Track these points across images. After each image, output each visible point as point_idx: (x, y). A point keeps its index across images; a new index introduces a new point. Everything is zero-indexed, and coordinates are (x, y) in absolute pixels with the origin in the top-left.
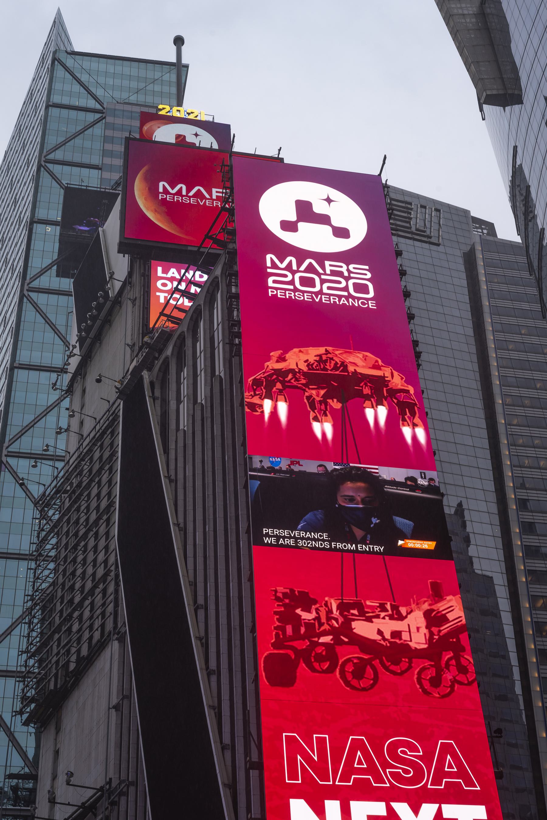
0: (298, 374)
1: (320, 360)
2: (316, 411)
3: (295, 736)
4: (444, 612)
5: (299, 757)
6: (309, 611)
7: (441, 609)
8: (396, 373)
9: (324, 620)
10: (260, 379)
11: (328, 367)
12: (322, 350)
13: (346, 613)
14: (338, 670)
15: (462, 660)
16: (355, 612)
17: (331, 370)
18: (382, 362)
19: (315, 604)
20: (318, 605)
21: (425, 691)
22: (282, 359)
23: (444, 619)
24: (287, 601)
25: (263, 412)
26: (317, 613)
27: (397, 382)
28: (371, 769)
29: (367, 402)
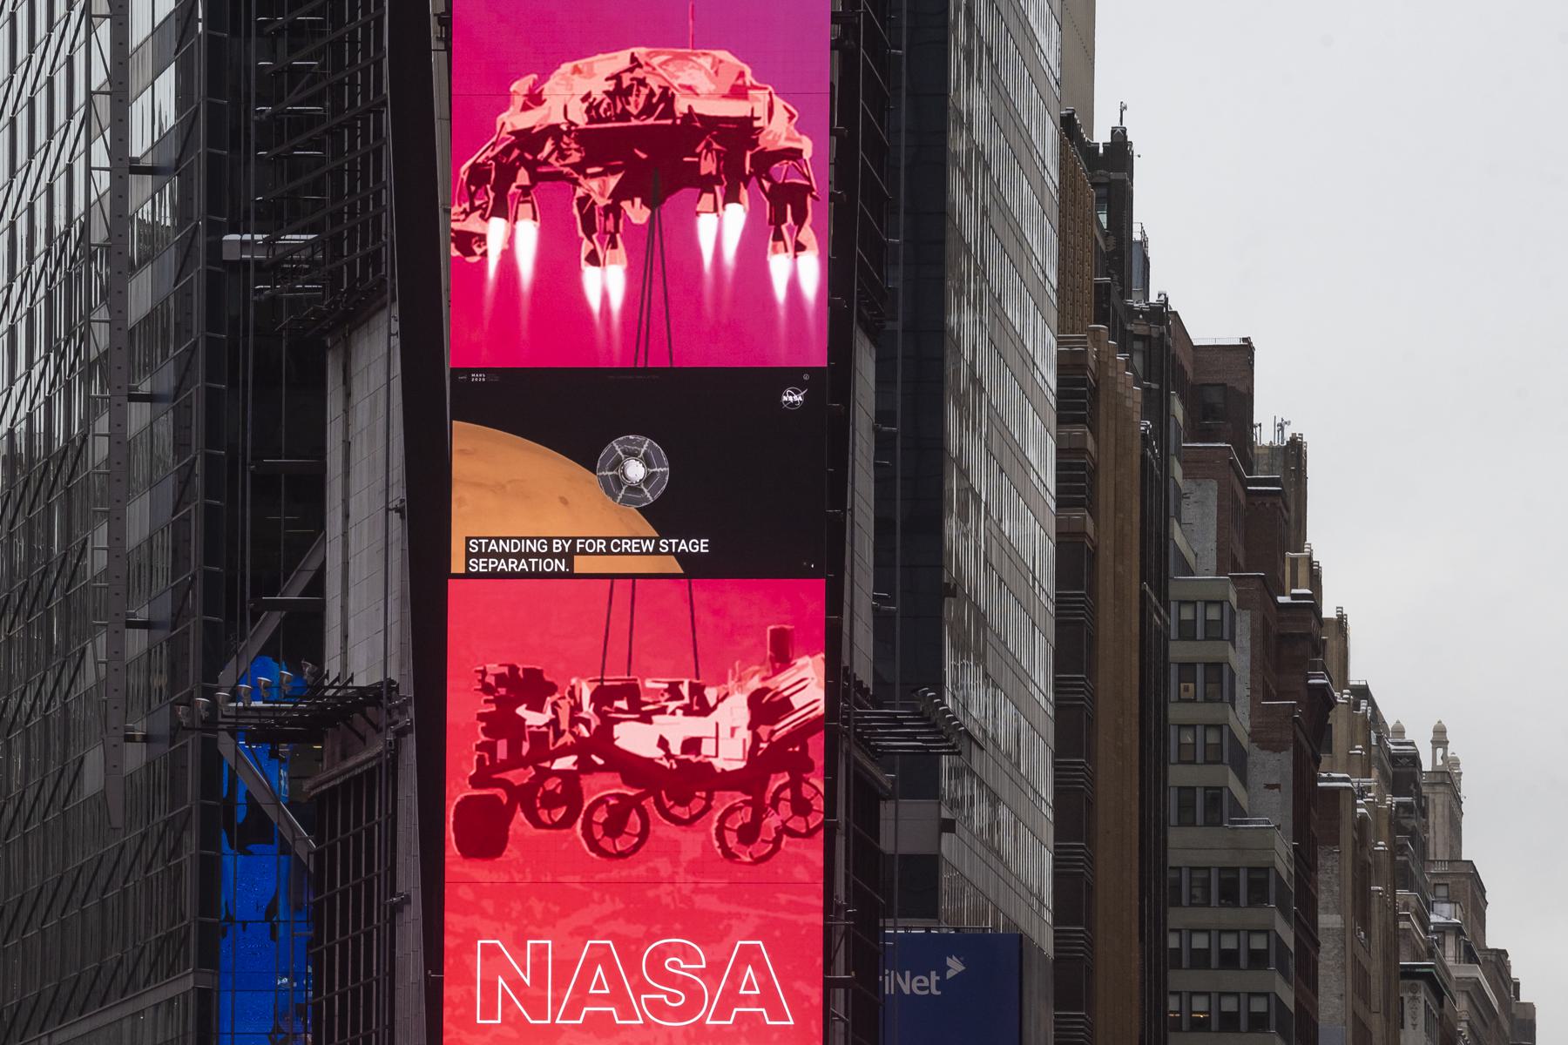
0: (566, 139)
1: (619, 92)
2: (594, 237)
3: (495, 945)
4: (786, 693)
5: (501, 981)
6: (537, 707)
7: (783, 687)
8: (779, 103)
9: (564, 725)
10: (484, 164)
11: (632, 109)
12: (621, 60)
13: (606, 708)
14: (579, 821)
15: (805, 788)
16: (622, 704)
17: (637, 117)
18: (753, 74)
19: (551, 694)
20: (557, 695)
21: (729, 854)
22: (534, 99)
23: (785, 706)
24: (502, 691)
25: (485, 254)
26: (554, 712)
27: (778, 131)
28: (618, 997)
29: (705, 196)
